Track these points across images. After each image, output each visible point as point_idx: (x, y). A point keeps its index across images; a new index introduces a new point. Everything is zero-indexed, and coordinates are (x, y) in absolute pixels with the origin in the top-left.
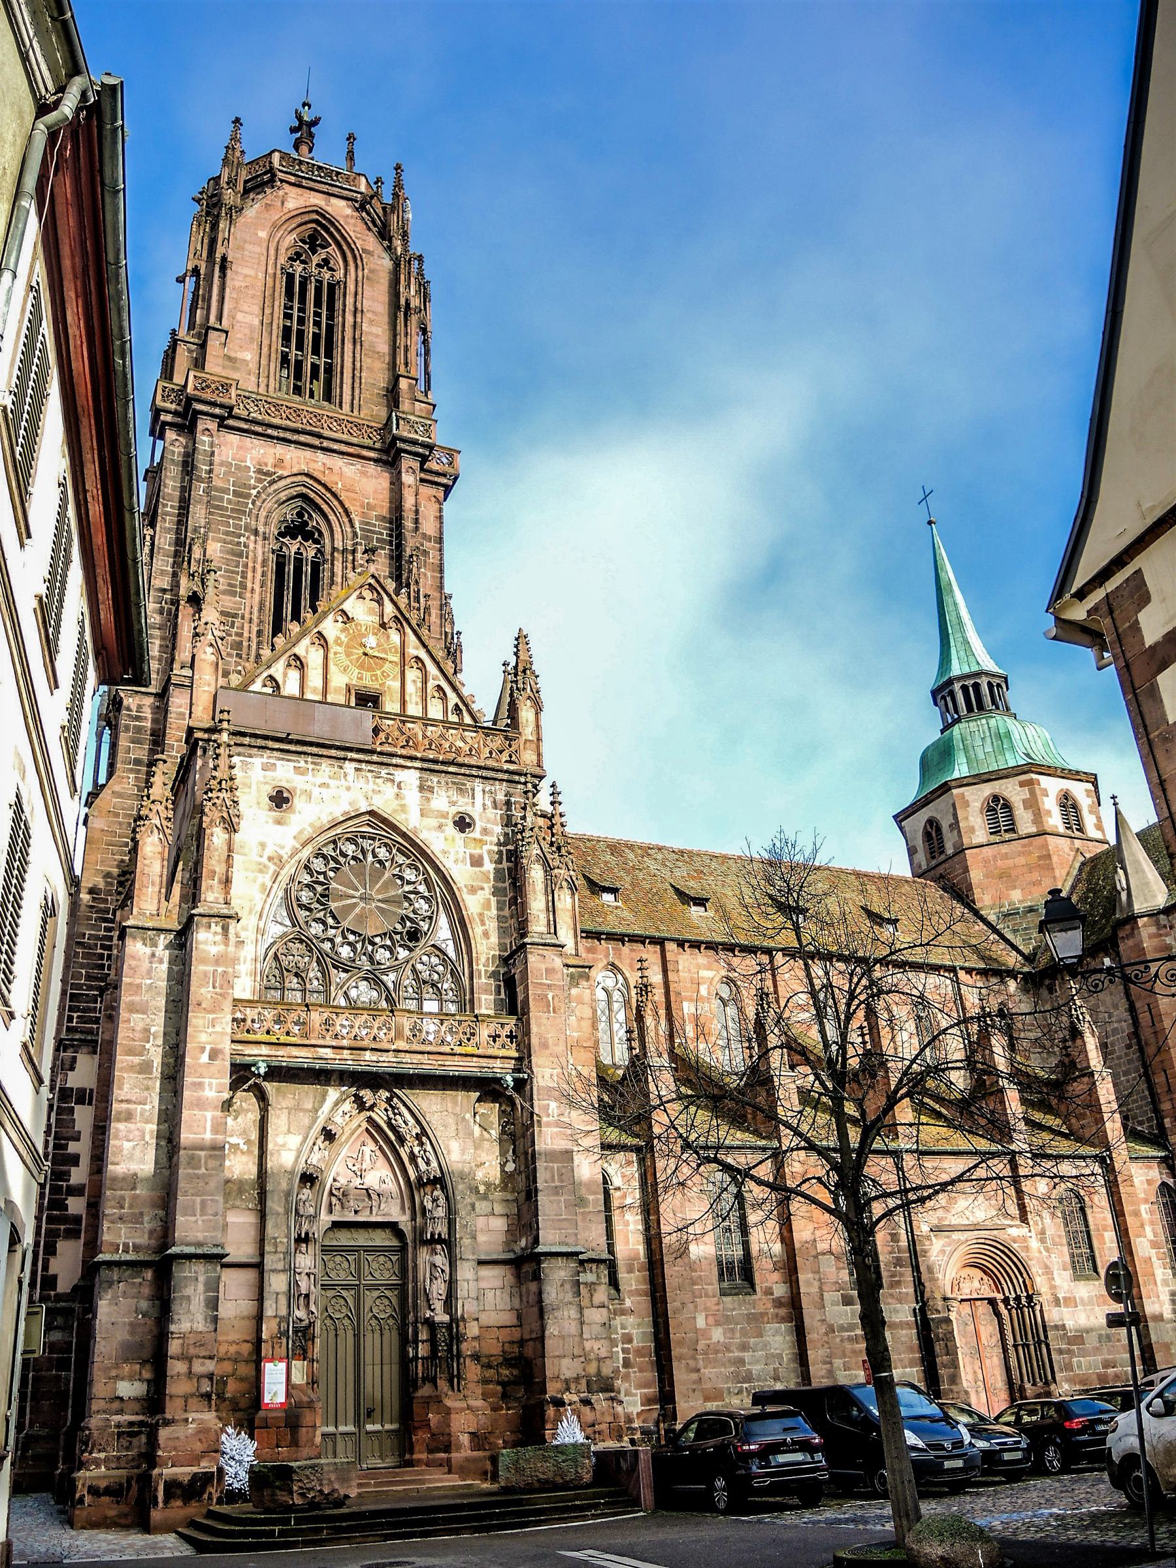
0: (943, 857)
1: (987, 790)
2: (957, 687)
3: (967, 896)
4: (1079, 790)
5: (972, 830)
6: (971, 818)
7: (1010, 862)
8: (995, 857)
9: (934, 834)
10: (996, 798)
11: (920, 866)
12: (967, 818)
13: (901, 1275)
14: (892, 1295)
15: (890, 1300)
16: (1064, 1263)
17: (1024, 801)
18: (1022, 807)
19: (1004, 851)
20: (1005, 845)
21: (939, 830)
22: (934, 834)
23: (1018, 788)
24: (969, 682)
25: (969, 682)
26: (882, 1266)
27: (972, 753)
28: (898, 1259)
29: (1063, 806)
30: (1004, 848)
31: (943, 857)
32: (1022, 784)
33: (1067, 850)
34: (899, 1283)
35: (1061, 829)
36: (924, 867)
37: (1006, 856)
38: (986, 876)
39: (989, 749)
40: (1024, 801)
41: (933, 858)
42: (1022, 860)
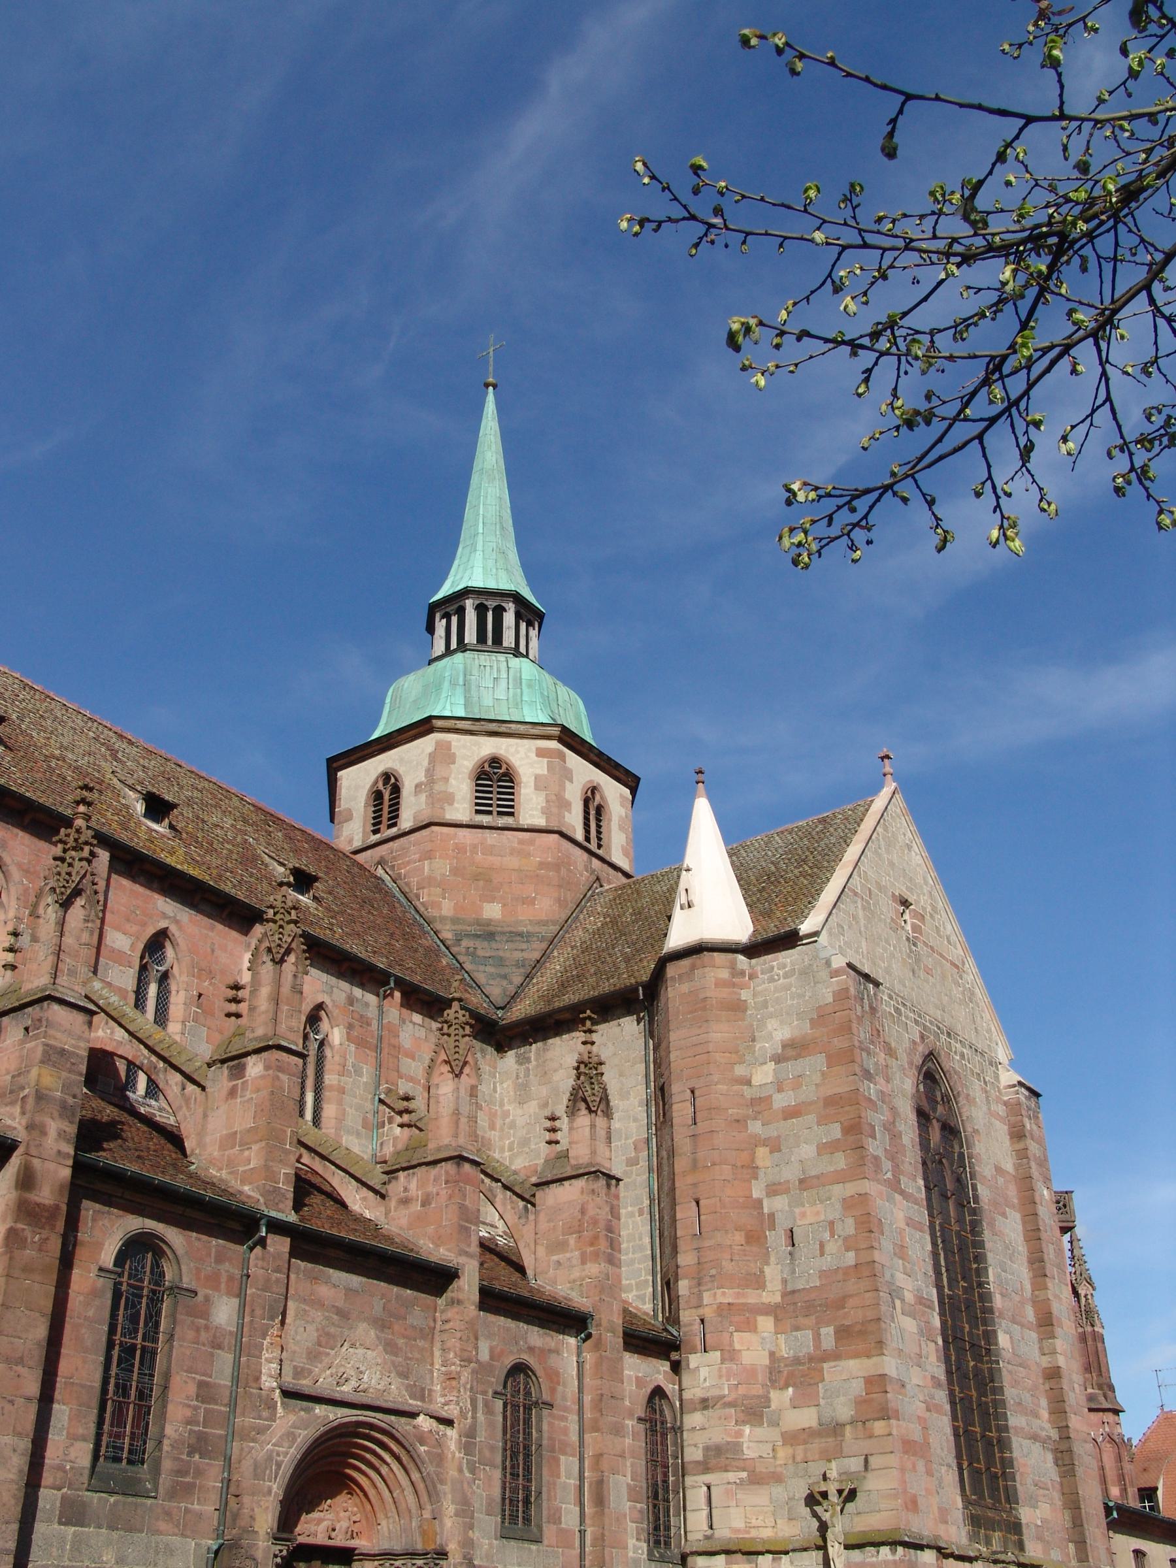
0: (394, 830)
1: (488, 746)
2: (469, 604)
3: (418, 896)
4: (613, 792)
5: (450, 799)
6: (452, 781)
7: (495, 860)
8: (474, 846)
9: (387, 797)
10: (495, 761)
11: (350, 841)
12: (446, 780)
13: (199, 1473)
14: (168, 1514)
15: (162, 1525)
16: (490, 1500)
17: (537, 778)
18: (532, 784)
19: (489, 842)
20: (495, 834)
21: (396, 790)
22: (387, 797)
23: (533, 755)
24: (491, 603)
25: (491, 603)
26: (166, 1446)
27: (474, 693)
28: (202, 1438)
29: (586, 802)
30: (491, 837)
31: (394, 830)
32: (541, 753)
33: (581, 867)
34: (188, 1489)
35: (579, 836)
36: (357, 843)
37: (490, 850)
38: (455, 871)
39: (501, 694)
40: (537, 778)
41: (375, 832)
42: (513, 862)
